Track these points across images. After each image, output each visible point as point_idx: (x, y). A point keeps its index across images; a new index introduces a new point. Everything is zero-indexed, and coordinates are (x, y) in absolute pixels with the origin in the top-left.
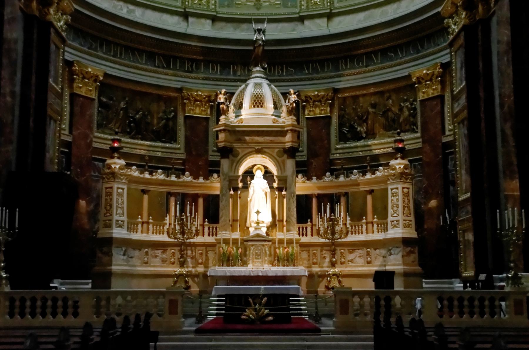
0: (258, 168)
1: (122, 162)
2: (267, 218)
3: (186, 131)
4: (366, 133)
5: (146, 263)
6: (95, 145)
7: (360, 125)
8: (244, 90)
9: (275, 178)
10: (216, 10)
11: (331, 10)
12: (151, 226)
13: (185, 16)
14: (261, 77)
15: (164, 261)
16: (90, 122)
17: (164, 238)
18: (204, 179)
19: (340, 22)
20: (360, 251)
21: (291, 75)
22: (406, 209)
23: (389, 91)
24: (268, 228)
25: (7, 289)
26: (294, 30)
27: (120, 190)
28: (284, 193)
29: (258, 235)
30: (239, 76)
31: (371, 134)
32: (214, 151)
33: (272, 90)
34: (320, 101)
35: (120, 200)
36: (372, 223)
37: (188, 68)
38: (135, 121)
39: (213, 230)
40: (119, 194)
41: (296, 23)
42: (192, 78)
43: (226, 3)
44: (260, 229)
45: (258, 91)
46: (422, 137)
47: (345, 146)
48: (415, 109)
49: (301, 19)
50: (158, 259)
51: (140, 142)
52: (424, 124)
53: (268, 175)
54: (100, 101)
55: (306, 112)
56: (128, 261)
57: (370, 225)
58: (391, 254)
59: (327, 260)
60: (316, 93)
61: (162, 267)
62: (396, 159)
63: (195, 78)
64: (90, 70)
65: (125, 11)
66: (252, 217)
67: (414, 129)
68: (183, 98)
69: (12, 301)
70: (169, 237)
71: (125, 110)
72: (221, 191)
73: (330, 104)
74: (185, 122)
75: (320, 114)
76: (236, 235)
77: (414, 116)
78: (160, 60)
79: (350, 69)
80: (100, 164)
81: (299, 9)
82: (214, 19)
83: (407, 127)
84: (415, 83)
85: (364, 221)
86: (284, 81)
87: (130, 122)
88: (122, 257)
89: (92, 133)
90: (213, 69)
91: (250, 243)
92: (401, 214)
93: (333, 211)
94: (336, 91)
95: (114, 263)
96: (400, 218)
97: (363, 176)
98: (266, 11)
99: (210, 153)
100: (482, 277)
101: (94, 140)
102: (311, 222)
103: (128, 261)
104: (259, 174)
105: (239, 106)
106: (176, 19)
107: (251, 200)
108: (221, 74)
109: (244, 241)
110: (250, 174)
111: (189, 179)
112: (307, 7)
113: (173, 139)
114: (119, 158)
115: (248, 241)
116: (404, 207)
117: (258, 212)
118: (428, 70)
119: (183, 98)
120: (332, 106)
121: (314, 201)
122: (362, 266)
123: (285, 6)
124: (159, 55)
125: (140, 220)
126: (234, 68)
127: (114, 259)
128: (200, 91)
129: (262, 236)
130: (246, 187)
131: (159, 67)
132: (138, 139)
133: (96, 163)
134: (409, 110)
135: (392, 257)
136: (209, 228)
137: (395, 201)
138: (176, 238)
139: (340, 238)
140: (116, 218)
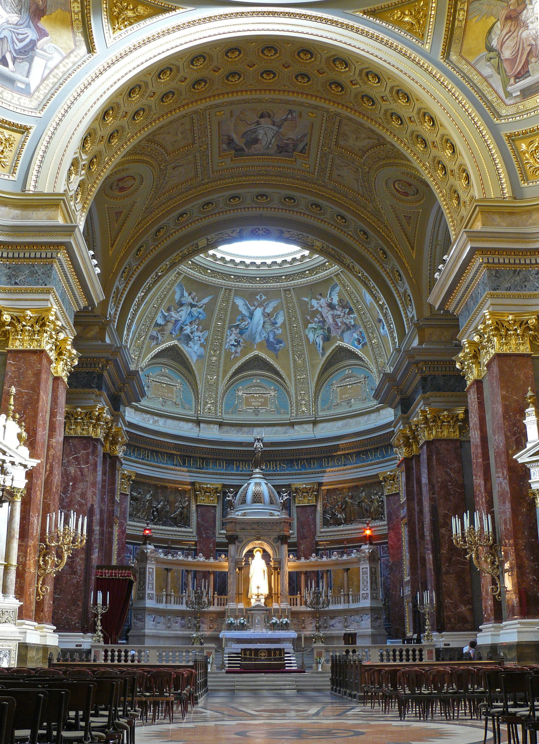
0: (257, 551)
1: (152, 547)
2: (265, 591)
3: (197, 517)
4: (345, 520)
5: (169, 628)
6: (128, 532)
7: (341, 513)
8: (247, 488)
9: (271, 559)
10: (222, 416)
11: (316, 418)
12: (173, 598)
13: (198, 422)
14: (260, 478)
15: (183, 626)
16: (125, 513)
17: (183, 607)
18: (214, 559)
19: (323, 428)
20: (339, 618)
21: (284, 470)
22: (374, 584)
23: (362, 486)
24: (266, 599)
25: (102, 644)
26: (286, 433)
27: (151, 570)
28: (278, 570)
29: (258, 606)
30: (241, 471)
31: (348, 521)
32: (220, 534)
33: (268, 487)
34: (307, 492)
35: (151, 578)
36: (348, 595)
37: (200, 465)
38: (157, 509)
39: (221, 601)
40: (149, 573)
41: (288, 427)
42: (203, 473)
43: (230, 410)
44: (260, 601)
45: (258, 488)
46: (388, 524)
47: (328, 530)
48: (382, 501)
49: (292, 425)
50: (178, 625)
51: (161, 527)
52: (390, 514)
53: (266, 556)
54: (131, 495)
55: (297, 501)
56: (156, 626)
57: (346, 597)
58: (362, 620)
59: (314, 625)
60: (304, 486)
61: (181, 630)
62: (366, 544)
63: (205, 473)
64: (126, 472)
65: (151, 421)
66: (253, 590)
67: (382, 518)
68: (195, 491)
69: (106, 651)
70: (187, 606)
71: (150, 501)
72: (229, 570)
73: (316, 495)
74: (197, 510)
75: (308, 503)
76: (241, 606)
77: (382, 508)
78: (177, 459)
79: (331, 467)
80: (131, 547)
81: (290, 415)
82: (221, 424)
83: (377, 517)
84: (382, 482)
85: (342, 593)
86: (278, 475)
87: (153, 512)
88: (152, 623)
89: (126, 522)
90: (220, 466)
91: (253, 612)
92: (369, 588)
93: (317, 585)
94: (320, 484)
95: (146, 627)
96: (369, 592)
97: (341, 557)
98: (263, 417)
99: (217, 535)
100: (415, 636)
101: (127, 527)
102: (300, 594)
103: (156, 626)
104: (258, 555)
105: (244, 501)
106: (190, 425)
107: (252, 576)
108: (226, 470)
109: (247, 610)
110: (250, 554)
111: (202, 559)
112: (297, 415)
113: (187, 524)
114: (150, 544)
115: (250, 610)
116: (372, 583)
117: (258, 588)
118: (391, 472)
119: (195, 491)
120: (317, 496)
121: (303, 577)
122: (341, 630)
123: (279, 413)
124: (177, 455)
125: (164, 593)
126: (236, 464)
127: (146, 624)
128: (209, 484)
129: (262, 607)
130: (248, 564)
131: (176, 465)
132: (159, 525)
133: (128, 546)
134: (378, 502)
135: (363, 622)
136: (218, 599)
137: (365, 578)
138: (193, 608)
139: (323, 608)
140: (148, 591)
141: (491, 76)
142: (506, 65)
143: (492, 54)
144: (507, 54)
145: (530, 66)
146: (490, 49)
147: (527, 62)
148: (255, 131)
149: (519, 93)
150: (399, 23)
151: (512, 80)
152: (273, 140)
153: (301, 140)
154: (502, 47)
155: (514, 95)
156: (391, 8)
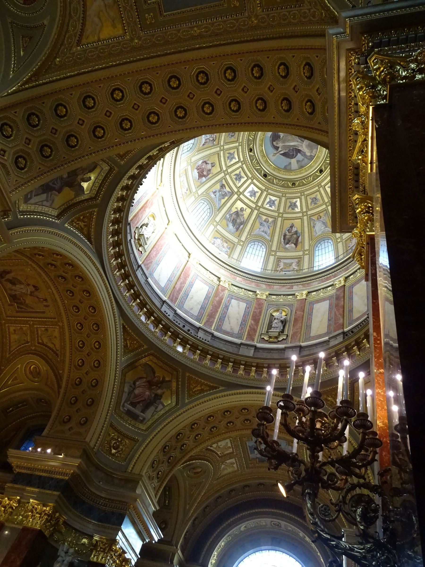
141: (126, 393)
142: (132, 395)
143: (133, 386)
144: (137, 392)
145: (138, 405)
146: (134, 383)
147: (139, 403)
148: (21, 283)
149: (126, 409)
150: (125, 340)
151: (129, 402)
152: (18, 292)
153: (27, 306)
154: (138, 387)
155: (125, 408)
156: (129, 334)
